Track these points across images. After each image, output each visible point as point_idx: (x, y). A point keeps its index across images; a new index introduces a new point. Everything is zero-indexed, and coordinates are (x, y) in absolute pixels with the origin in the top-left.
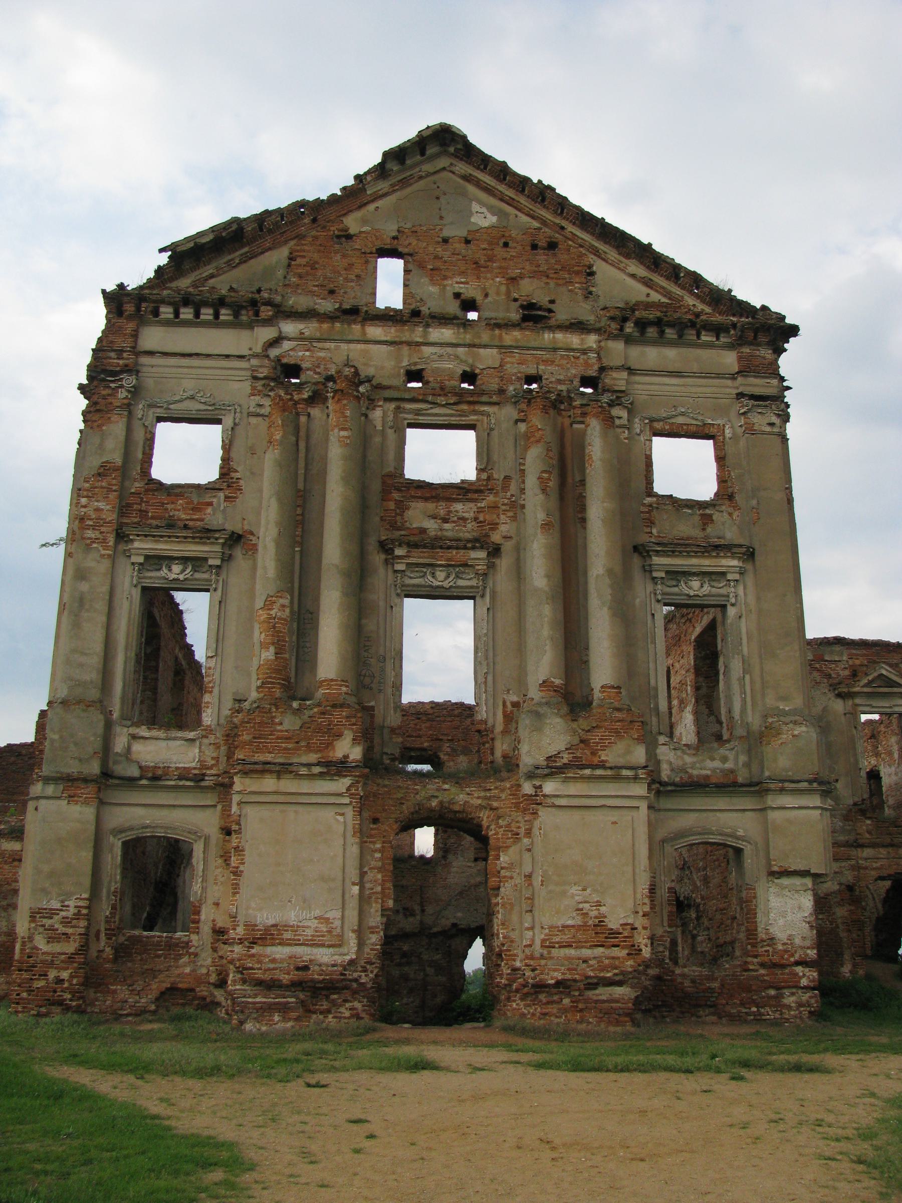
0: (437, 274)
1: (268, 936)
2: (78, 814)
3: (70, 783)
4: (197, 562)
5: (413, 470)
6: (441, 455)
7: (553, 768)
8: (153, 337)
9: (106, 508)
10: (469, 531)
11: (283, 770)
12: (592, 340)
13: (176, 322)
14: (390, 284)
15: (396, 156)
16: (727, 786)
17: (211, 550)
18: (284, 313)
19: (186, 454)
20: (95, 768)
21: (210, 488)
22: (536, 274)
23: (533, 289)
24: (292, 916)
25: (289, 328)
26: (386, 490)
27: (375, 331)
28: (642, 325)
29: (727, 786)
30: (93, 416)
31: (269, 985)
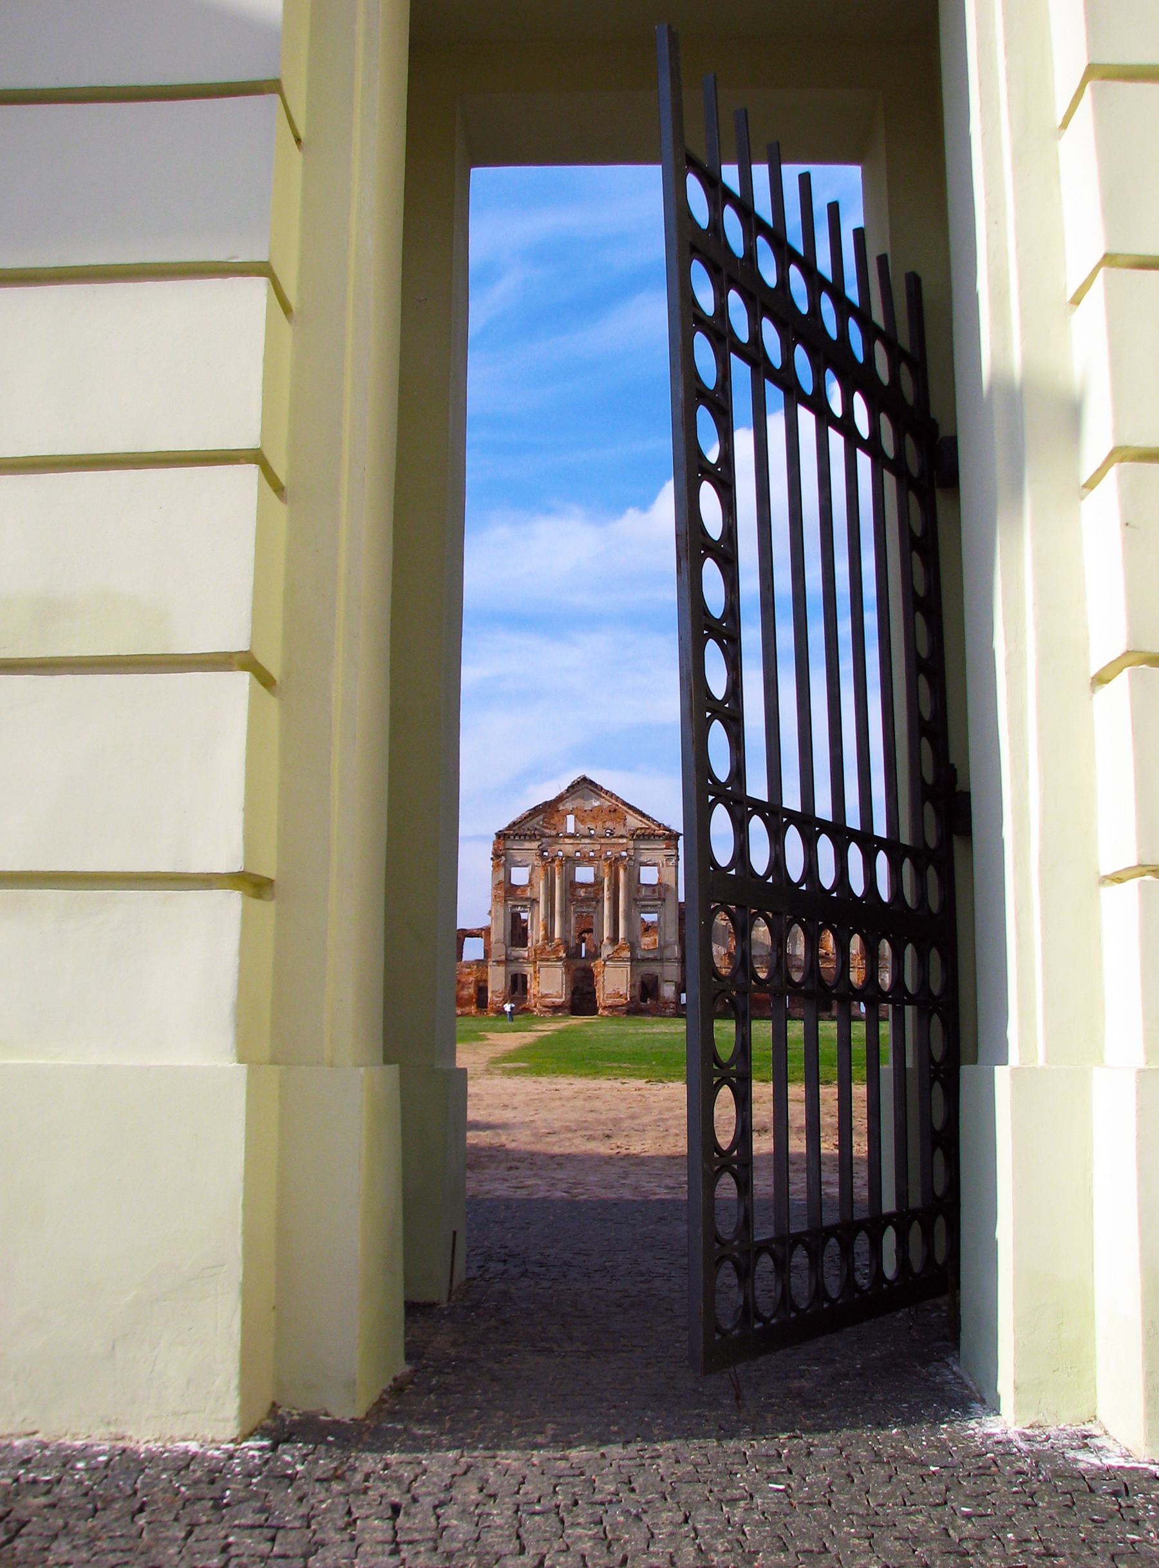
0: (583, 822)
1: (546, 996)
2: (501, 969)
3: (499, 962)
4: (525, 906)
5: (578, 879)
6: (584, 874)
7: (609, 958)
8: (509, 844)
9: (501, 893)
10: (592, 895)
11: (548, 960)
12: (625, 841)
13: (514, 839)
14: (571, 824)
15: (572, 786)
16: (654, 960)
17: (527, 903)
18: (543, 836)
19: (520, 876)
20: (503, 958)
21: (527, 886)
22: (612, 820)
23: (609, 824)
24: (550, 992)
25: (544, 840)
26: (571, 886)
27: (567, 841)
28: (638, 836)
29: (654, 960)
30: (496, 867)
31: (546, 1007)
